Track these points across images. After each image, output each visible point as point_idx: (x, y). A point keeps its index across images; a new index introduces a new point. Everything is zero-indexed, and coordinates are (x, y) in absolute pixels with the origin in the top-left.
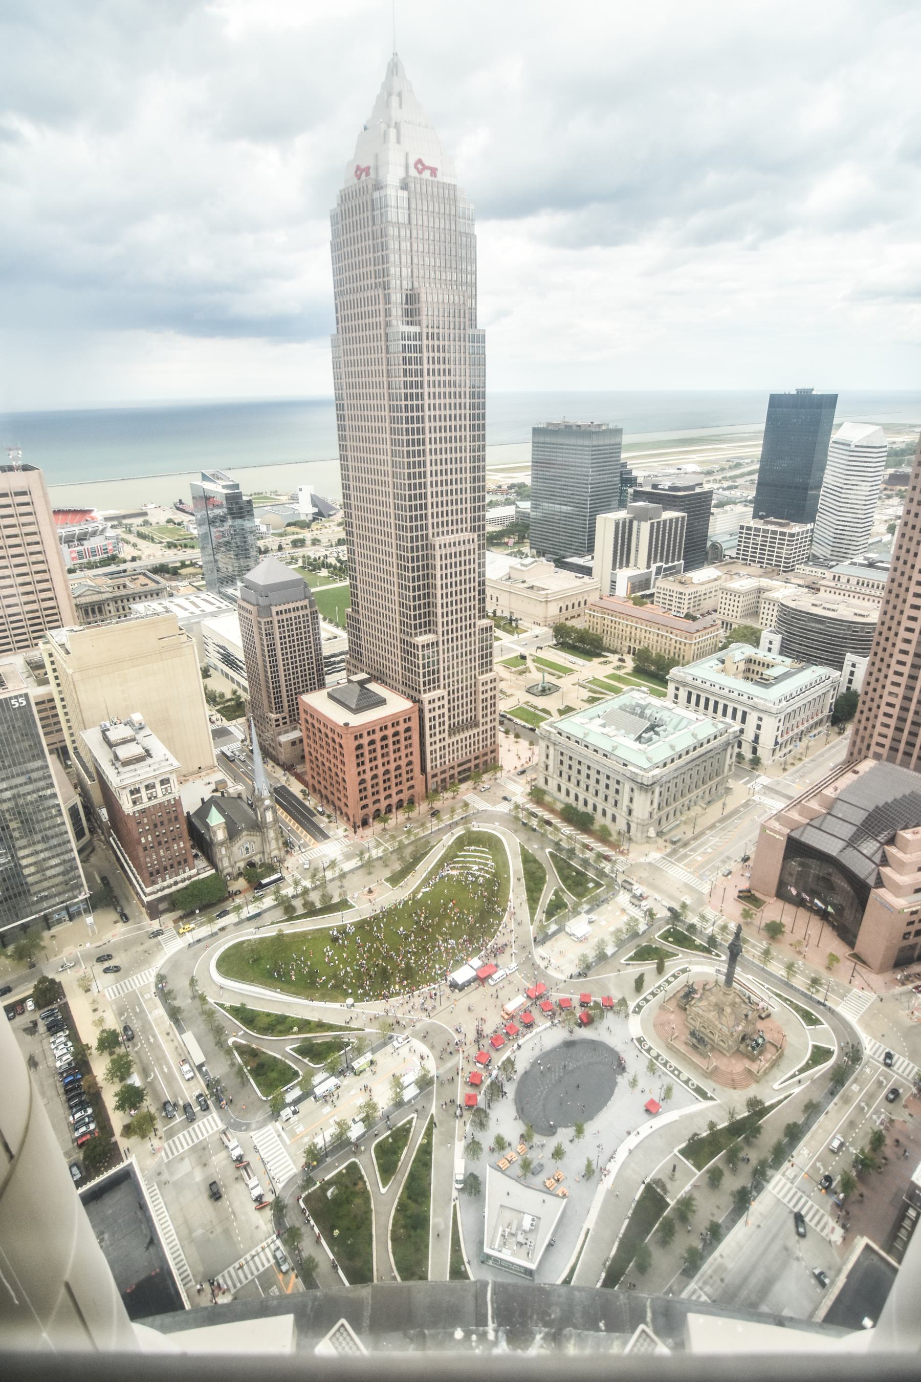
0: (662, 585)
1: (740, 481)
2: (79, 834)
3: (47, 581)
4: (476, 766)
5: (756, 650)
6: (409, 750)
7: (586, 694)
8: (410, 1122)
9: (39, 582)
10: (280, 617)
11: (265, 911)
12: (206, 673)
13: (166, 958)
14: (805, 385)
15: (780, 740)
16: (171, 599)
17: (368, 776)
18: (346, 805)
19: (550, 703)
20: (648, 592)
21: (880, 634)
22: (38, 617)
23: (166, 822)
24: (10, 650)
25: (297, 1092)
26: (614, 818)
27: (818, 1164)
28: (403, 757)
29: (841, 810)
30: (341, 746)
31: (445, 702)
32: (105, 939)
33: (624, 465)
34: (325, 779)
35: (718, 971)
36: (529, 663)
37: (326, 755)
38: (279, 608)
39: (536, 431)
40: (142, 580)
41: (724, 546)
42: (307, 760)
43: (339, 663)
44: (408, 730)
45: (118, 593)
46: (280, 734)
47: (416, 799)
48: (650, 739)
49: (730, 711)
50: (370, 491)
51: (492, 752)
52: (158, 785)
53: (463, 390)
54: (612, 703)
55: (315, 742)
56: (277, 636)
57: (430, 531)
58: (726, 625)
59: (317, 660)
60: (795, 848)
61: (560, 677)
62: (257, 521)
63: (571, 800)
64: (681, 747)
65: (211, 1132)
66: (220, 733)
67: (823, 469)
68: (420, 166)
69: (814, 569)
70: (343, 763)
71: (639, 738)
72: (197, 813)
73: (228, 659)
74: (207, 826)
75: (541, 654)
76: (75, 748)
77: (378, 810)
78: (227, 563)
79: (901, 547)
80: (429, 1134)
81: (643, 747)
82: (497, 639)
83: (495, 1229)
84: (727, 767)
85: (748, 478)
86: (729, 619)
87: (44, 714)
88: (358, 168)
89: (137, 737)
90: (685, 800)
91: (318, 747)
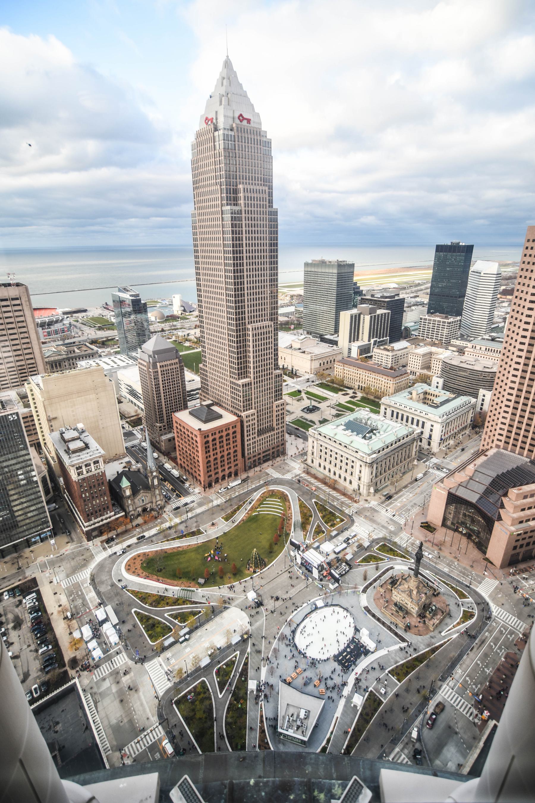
0: (377, 352)
1: (419, 293)
2: (47, 492)
3: (29, 348)
4: (273, 453)
5: (429, 387)
6: (235, 444)
7: (334, 412)
8: (235, 657)
9: (25, 349)
10: (162, 369)
11: (153, 536)
12: (120, 402)
13: (96, 563)
14: (455, 241)
15: (443, 437)
16: (101, 359)
17: (212, 459)
18: (199, 475)
19: (314, 417)
20: (369, 355)
21: (499, 378)
24: (8, 387)
25: (171, 640)
26: (351, 482)
27: (467, 678)
28: (232, 447)
29: (479, 477)
30: (196, 442)
31: (256, 417)
32: (61, 553)
33: (355, 284)
34: (187, 460)
35: (409, 568)
36: (303, 395)
37: (188, 447)
38: (162, 364)
39: (307, 265)
40: (84, 348)
41: (411, 329)
43: (196, 394)
44: (234, 432)
45: (70, 356)
46: (162, 435)
47: (239, 472)
48: (371, 438)
49: (415, 421)
50: (214, 298)
51: (282, 444)
52: (92, 465)
53: (265, 242)
54: (350, 417)
55: (182, 439)
56: (160, 380)
57: (247, 321)
58: (414, 373)
59: (183, 393)
60: (453, 499)
61: (320, 403)
62: (149, 315)
63: (326, 472)
64: (388, 441)
65: (121, 663)
66: (128, 435)
67: (466, 286)
68: (241, 118)
69: (462, 342)
70: (197, 451)
71: (364, 437)
73: (133, 393)
74: (120, 487)
75: (310, 390)
76: (45, 443)
77: (217, 478)
78: (132, 337)
79: (509, 330)
80: (246, 664)
81: (368, 441)
82: (285, 381)
83: (284, 717)
84: (414, 453)
85: (425, 291)
86: (415, 370)
87: (27, 424)
88: (207, 119)
90: (391, 472)
91: (183, 443)
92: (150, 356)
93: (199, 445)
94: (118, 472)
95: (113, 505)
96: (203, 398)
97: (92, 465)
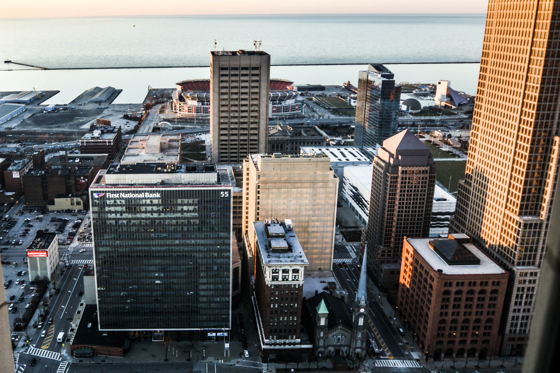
3: (256, 123)
9: (252, 123)
10: (404, 176)
12: (339, 205)
18: (424, 335)
22: (246, 144)
23: (289, 299)
24: (226, 161)
34: (411, 308)
37: (417, 290)
38: (405, 169)
42: (400, 289)
46: (383, 262)
52: (291, 272)
72: (311, 299)
89: (286, 235)
92: (391, 155)
93: (434, 293)
94: (317, 292)
95: (302, 331)
96: (455, 228)
97: (291, 272)
